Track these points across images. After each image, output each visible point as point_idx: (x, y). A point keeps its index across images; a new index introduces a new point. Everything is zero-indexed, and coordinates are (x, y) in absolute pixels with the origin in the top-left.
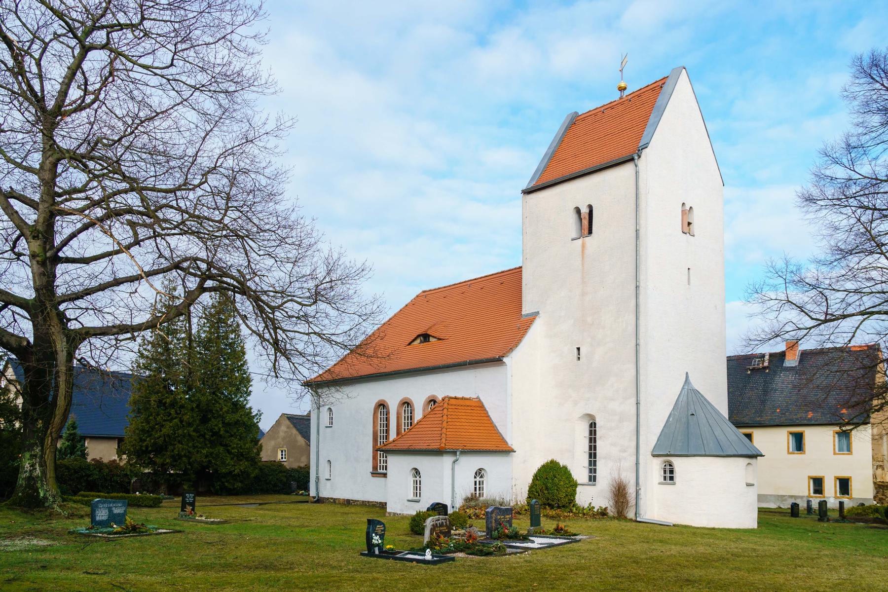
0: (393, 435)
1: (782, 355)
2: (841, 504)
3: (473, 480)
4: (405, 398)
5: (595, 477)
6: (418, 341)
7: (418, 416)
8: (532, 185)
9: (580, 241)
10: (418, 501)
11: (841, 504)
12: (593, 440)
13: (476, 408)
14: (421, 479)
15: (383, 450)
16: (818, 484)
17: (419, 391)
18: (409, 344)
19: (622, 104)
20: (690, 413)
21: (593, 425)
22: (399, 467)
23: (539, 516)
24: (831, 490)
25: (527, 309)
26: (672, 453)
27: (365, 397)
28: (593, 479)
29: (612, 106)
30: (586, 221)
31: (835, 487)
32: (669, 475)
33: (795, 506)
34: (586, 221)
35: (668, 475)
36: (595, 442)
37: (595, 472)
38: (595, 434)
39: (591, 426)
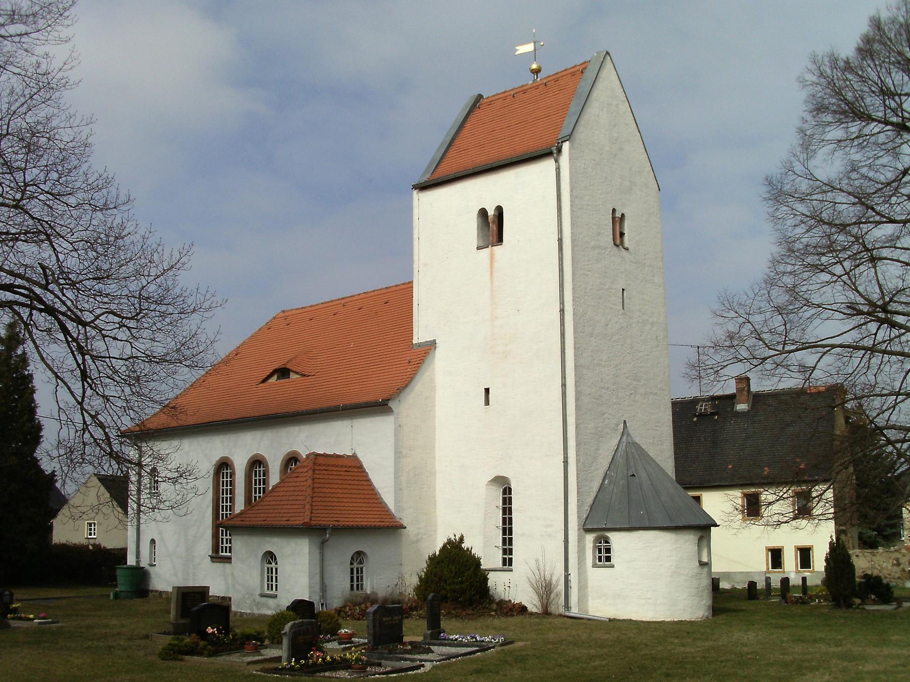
0: (240, 505)
1: (731, 398)
2: (804, 579)
3: (349, 567)
4: (256, 455)
5: (510, 560)
6: (275, 377)
7: (274, 479)
8: (425, 179)
9: (486, 251)
10: (275, 597)
11: (804, 579)
12: (507, 510)
13: (350, 470)
14: (278, 566)
15: (226, 527)
16: (776, 556)
17: (273, 446)
18: (264, 381)
19: (537, 87)
20: (631, 473)
21: (507, 491)
22: (246, 551)
23: (439, 615)
24: (790, 561)
25: (420, 336)
26: (609, 526)
27: (198, 455)
28: (508, 562)
29: (524, 90)
30: (492, 226)
31: (796, 559)
32: (604, 555)
33: (752, 585)
34: (492, 226)
35: (604, 554)
36: (510, 513)
37: (511, 553)
38: (510, 503)
39: (504, 492)
